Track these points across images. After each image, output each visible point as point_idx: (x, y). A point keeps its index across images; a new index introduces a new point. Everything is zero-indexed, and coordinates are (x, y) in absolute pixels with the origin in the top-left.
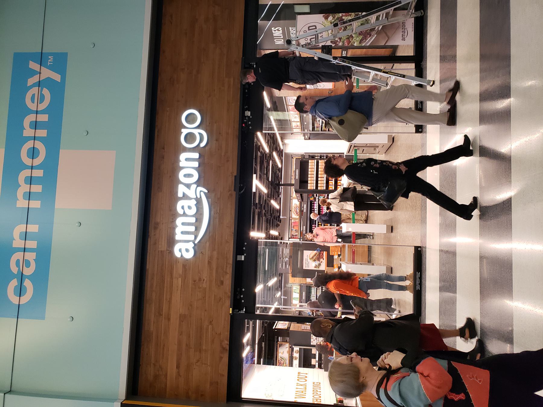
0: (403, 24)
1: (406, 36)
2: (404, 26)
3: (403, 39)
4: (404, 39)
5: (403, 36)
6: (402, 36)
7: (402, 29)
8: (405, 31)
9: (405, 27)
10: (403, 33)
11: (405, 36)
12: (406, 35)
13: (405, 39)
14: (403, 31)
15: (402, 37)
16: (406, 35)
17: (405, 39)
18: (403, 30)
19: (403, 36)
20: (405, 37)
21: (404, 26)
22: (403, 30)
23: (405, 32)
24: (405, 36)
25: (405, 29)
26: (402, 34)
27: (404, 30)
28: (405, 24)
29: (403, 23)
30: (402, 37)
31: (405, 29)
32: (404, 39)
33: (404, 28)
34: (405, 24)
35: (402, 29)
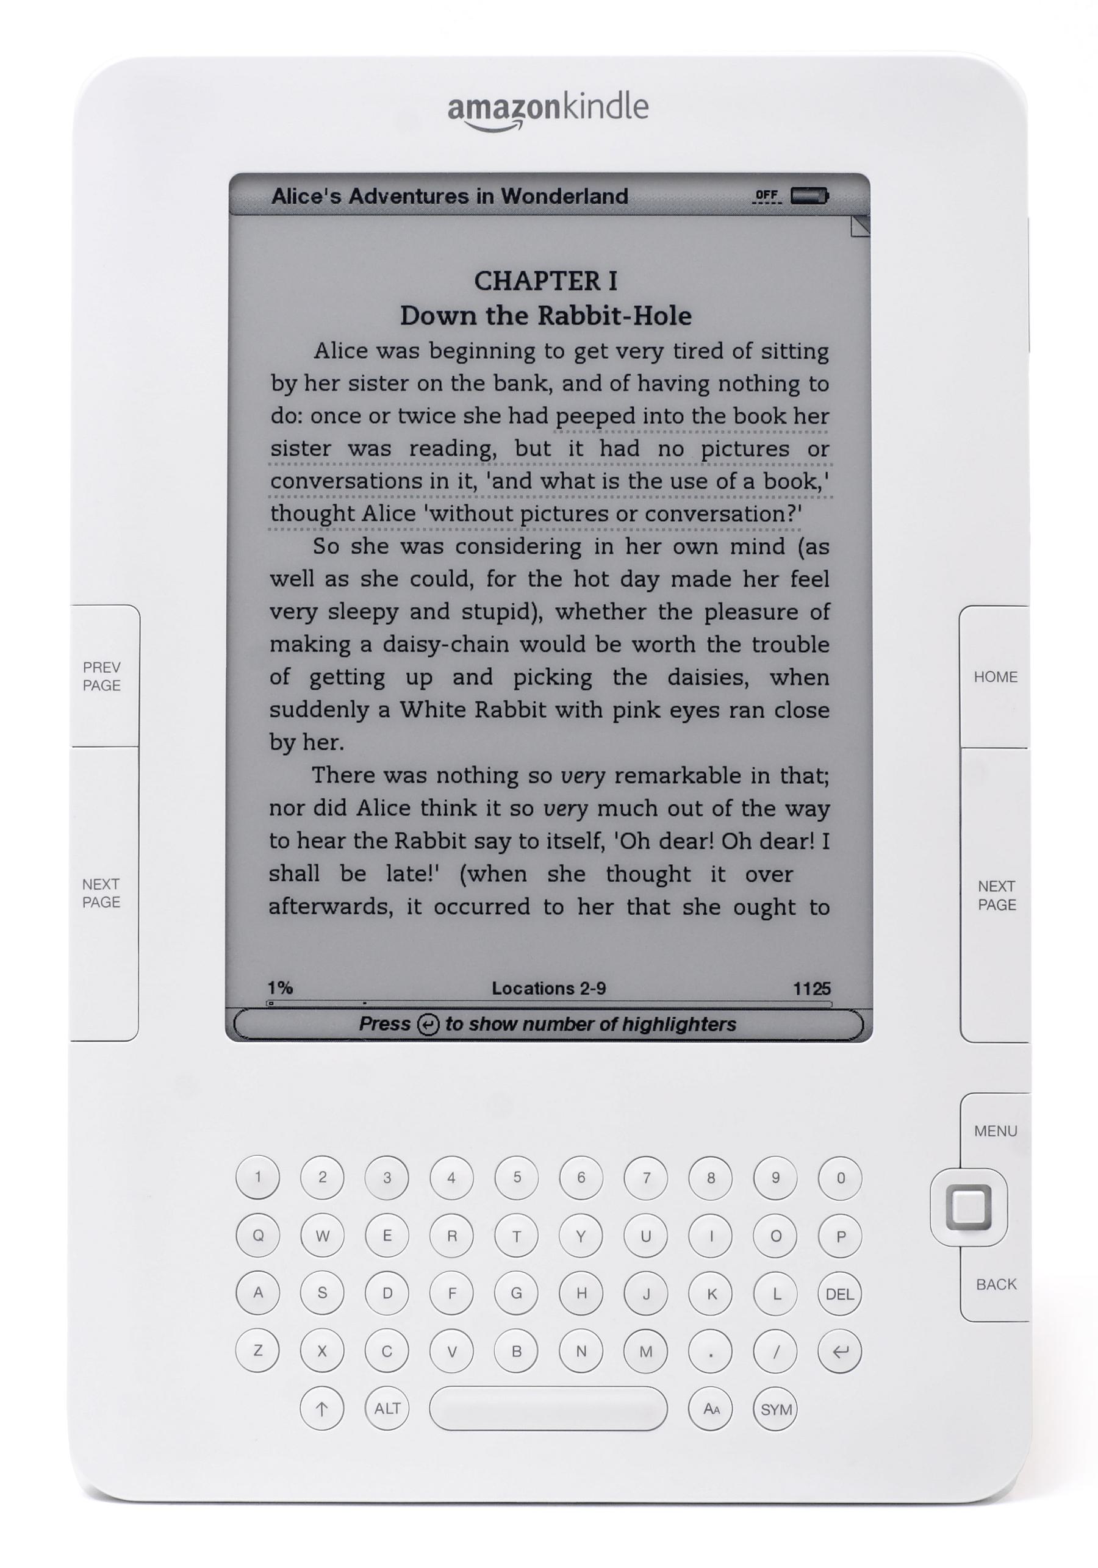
0: (548, 103)
2: (535, 111)
3: (460, 109)
5: (474, 107)
6: (477, 102)
7: (515, 102)
8: (506, 115)
9: (527, 120)
10: (493, 108)
11: (479, 116)
12: (483, 122)
13: (461, 115)
15: (470, 103)
16: (483, 122)
17: (461, 115)
18: (512, 108)
19: (474, 107)
20: (470, 116)
21: (535, 111)
22: (512, 108)
23: (496, 115)
24: (479, 116)
25: (513, 116)
28: (548, 116)
29: (553, 107)
30: (470, 103)
31: (513, 116)
32: (456, 113)
33: (524, 110)
34: (548, 116)
35: (515, 102)
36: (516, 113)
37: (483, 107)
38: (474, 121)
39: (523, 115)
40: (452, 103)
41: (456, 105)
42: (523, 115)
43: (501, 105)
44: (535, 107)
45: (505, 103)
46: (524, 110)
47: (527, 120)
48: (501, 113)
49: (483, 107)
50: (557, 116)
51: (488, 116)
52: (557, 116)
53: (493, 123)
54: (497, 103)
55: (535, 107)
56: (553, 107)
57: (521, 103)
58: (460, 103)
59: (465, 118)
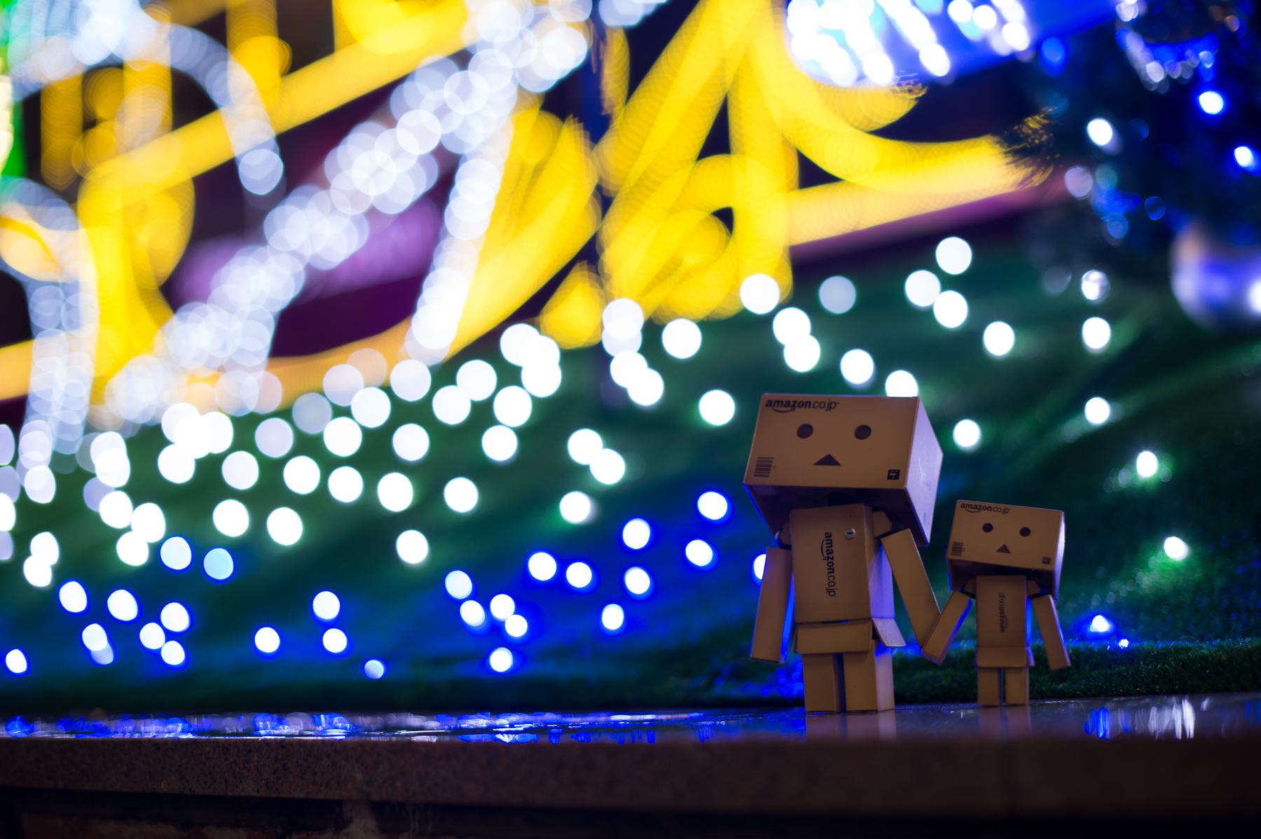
0: (833, 569)
1: (825, 542)
3: (828, 537)
5: (829, 542)
6: (831, 543)
8: (828, 554)
9: (826, 562)
10: (830, 549)
12: (824, 546)
15: (831, 540)
16: (824, 546)
17: (826, 537)
18: (830, 556)
19: (829, 542)
22: (830, 556)
23: (827, 550)
24: (827, 544)
26: (832, 546)
27: (829, 555)
28: (828, 569)
29: (831, 571)
30: (831, 540)
33: (830, 560)
34: (828, 569)
36: (828, 558)
38: (825, 542)
44: (831, 564)
45: (832, 553)
46: (830, 560)
47: (826, 562)
50: (829, 573)
51: (827, 547)
52: (829, 573)
53: (825, 549)
54: (832, 550)
55: (831, 564)
56: (831, 571)
57: (832, 559)
58: (831, 536)
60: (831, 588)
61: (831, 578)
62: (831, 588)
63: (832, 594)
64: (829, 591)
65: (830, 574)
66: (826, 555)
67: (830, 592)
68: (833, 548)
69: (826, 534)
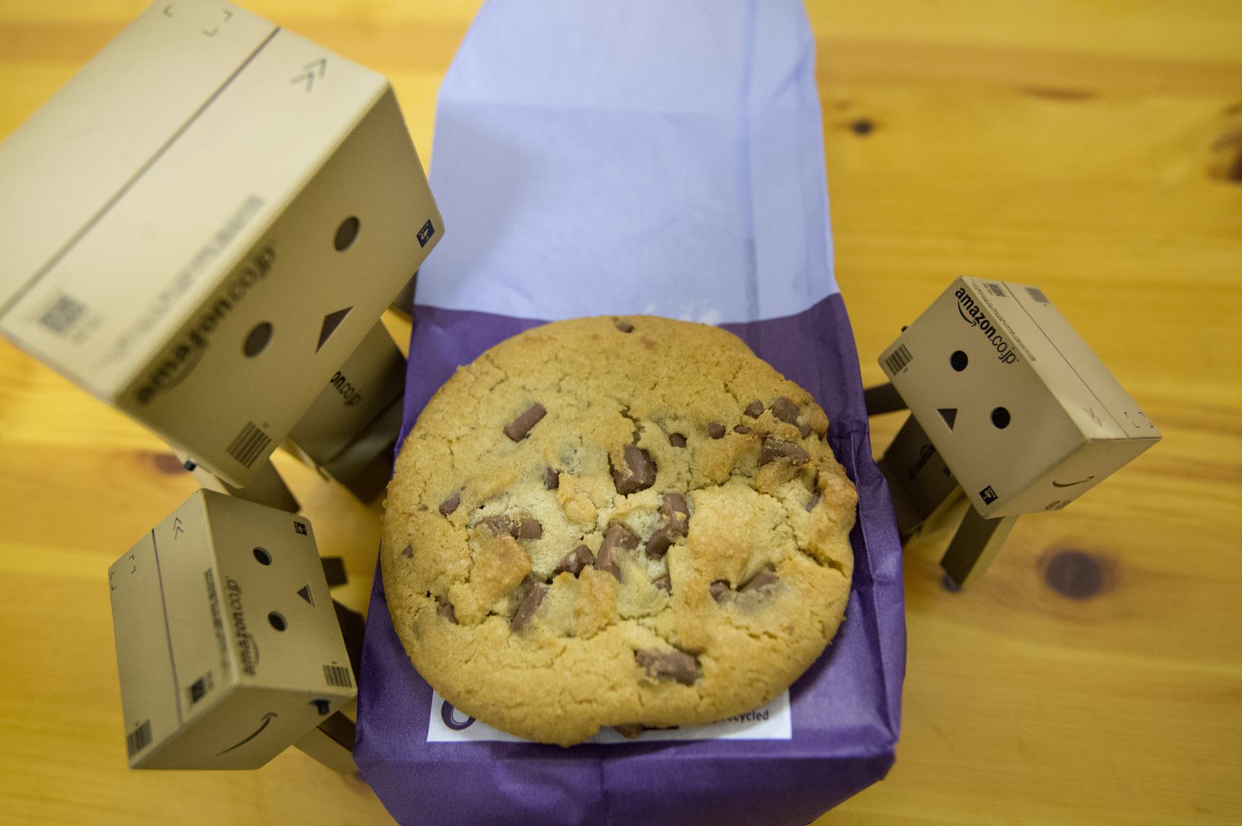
0: (992, 328)
1: (962, 304)
3: (962, 294)
4: (959, 294)
5: (967, 300)
6: (970, 300)
7: (982, 314)
8: (973, 315)
9: (978, 326)
10: (972, 307)
11: (965, 305)
12: (964, 309)
14: (976, 312)
16: (964, 309)
17: (960, 297)
18: (978, 315)
19: (967, 300)
20: (962, 301)
22: (978, 315)
23: (970, 312)
24: (965, 305)
26: (973, 303)
28: (986, 333)
29: (991, 332)
30: (967, 296)
32: (959, 294)
33: (981, 321)
34: (986, 333)
35: (982, 314)
36: (977, 319)
37: (970, 303)
38: (962, 304)
39: (979, 323)
40: (962, 289)
41: (962, 291)
42: (979, 323)
43: (976, 310)
46: (981, 321)
47: (978, 326)
48: (973, 312)
49: (970, 303)
50: (989, 337)
51: (968, 308)
52: (989, 337)
53: (966, 313)
54: (976, 307)
56: (991, 332)
57: (983, 317)
58: (964, 292)
59: (960, 300)
60: (1004, 353)
61: (997, 341)
62: (1004, 353)
63: (1009, 360)
64: (1005, 359)
65: (992, 338)
66: (971, 319)
67: (1007, 359)
68: (974, 305)
69: (957, 294)
